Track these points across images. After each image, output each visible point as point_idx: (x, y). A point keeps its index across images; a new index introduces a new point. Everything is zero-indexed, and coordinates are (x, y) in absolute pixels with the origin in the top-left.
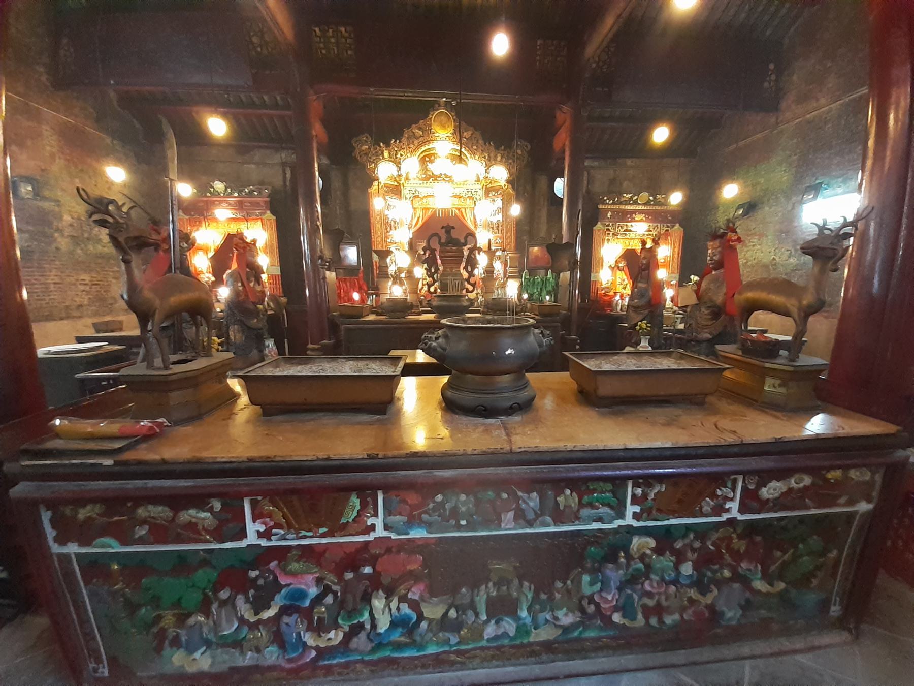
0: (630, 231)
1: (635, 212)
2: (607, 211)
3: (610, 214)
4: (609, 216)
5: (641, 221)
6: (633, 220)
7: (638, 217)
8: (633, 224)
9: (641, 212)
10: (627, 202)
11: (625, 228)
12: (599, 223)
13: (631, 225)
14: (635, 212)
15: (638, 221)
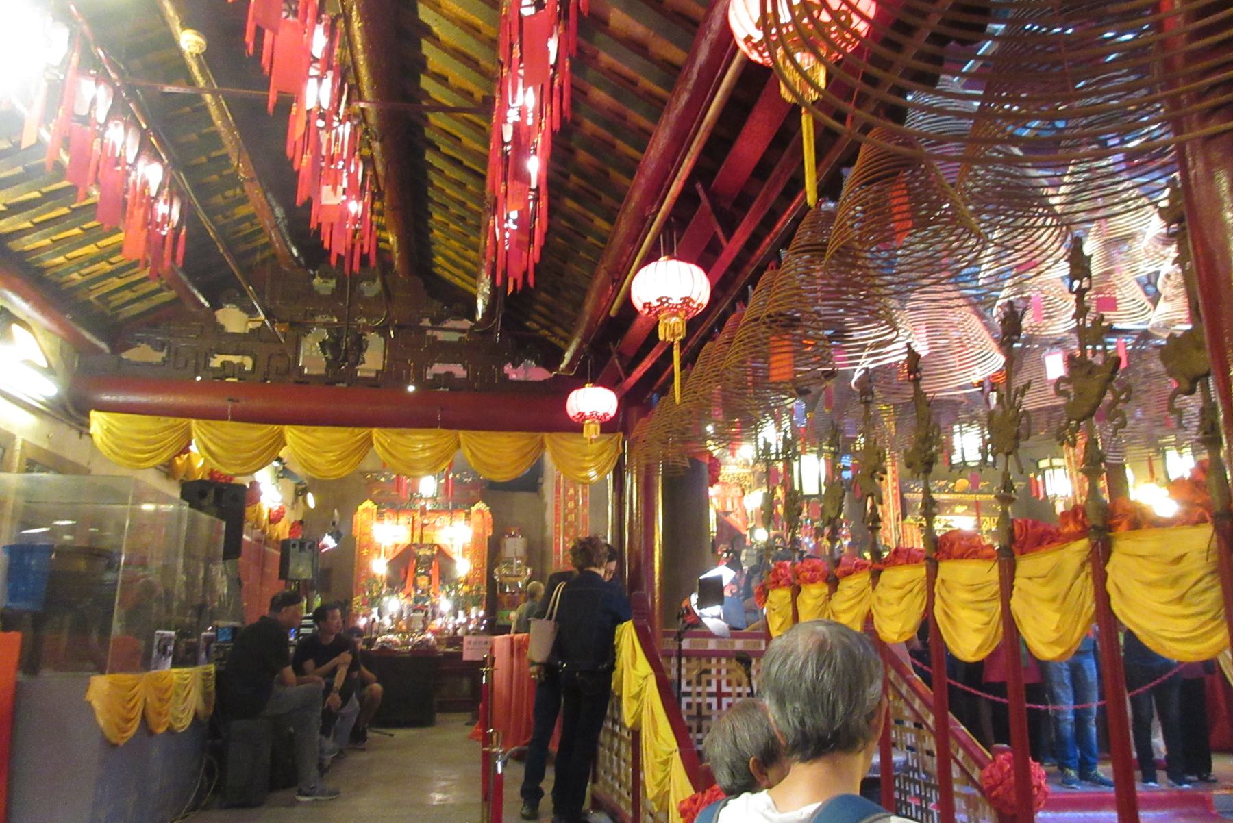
1: (951, 504)
6: (952, 513)
7: (960, 509)
9: (962, 503)
15: (958, 514)
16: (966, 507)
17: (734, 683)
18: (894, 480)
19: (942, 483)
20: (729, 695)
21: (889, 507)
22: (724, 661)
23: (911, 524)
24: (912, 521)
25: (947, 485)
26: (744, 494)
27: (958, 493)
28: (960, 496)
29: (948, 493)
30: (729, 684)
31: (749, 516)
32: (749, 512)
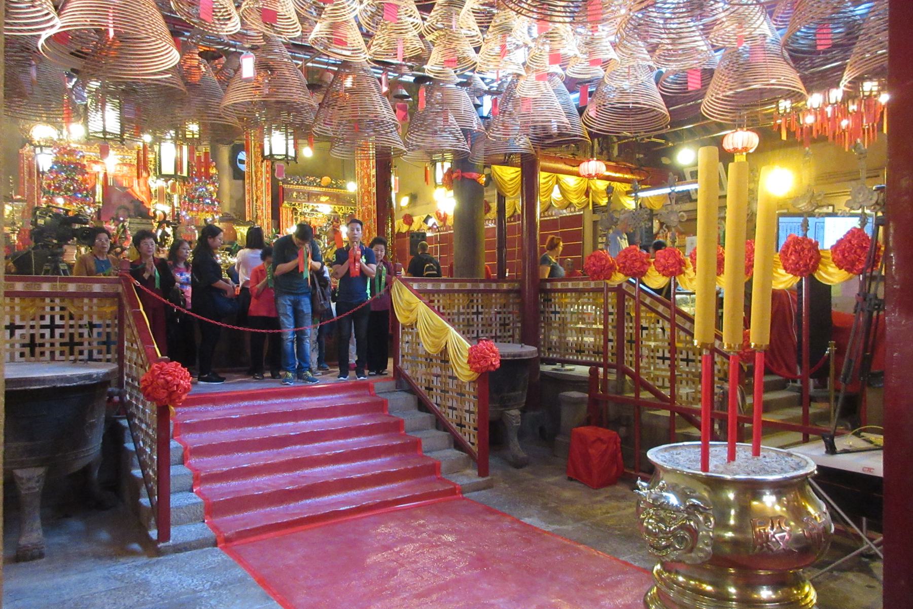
0: (316, 211)
1: (317, 195)
2: (292, 191)
3: (295, 194)
4: (294, 196)
5: (326, 202)
6: (318, 201)
7: (323, 199)
8: (319, 205)
9: (325, 194)
10: (311, 184)
11: (311, 209)
12: (285, 202)
13: (318, 207)
14: (317, 195)
15: (322, 202)
16: (328, 198)
17: (67, 317)
18: (267, 172)
19: (312, 179)
20: (43, 327)
21: (262, 193)
22: (57, 301)
23: (286, 208)
24: (287, 205)
25: (315, 180)
26: (149, 175)
27: (323, 187)
28: (324, 189)
29: (316, 186)
30: (62, 318)
31: (153, 193)
32: (153, 190)
